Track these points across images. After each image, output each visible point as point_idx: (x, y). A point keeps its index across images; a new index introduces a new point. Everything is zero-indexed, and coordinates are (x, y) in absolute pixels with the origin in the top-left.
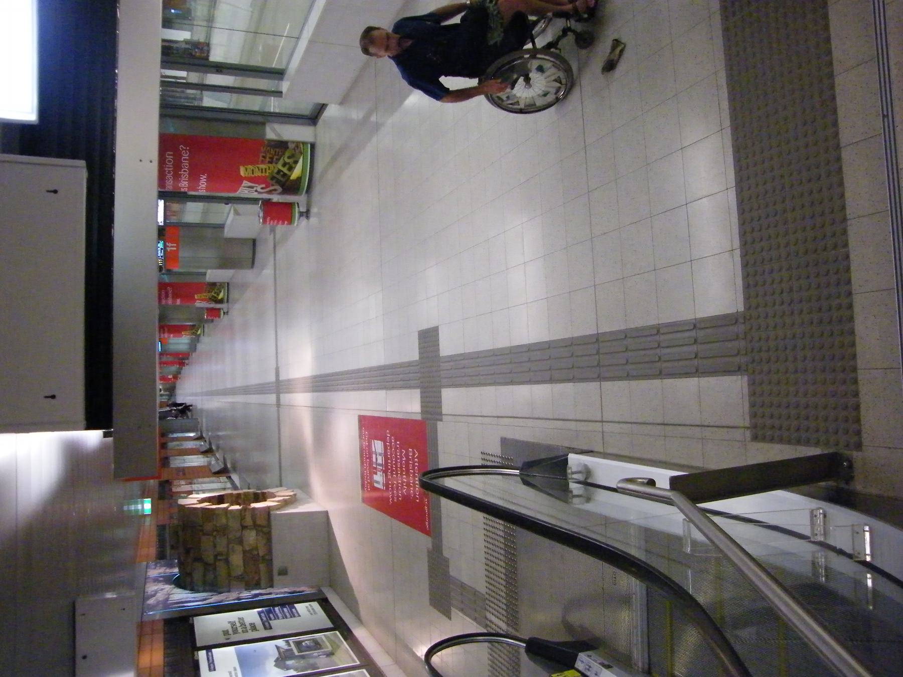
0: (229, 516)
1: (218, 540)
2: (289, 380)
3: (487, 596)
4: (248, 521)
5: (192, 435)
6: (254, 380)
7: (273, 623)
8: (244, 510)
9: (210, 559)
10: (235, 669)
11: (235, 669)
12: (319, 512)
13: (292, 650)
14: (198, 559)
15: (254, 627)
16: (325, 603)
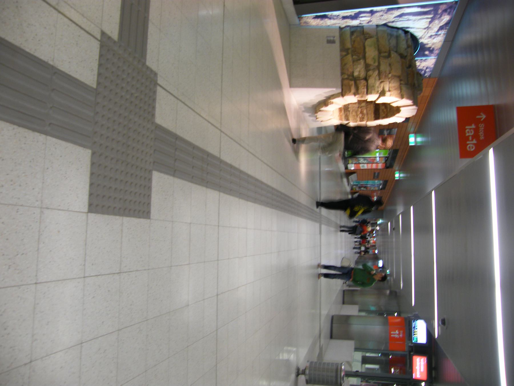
9: (394, 55)
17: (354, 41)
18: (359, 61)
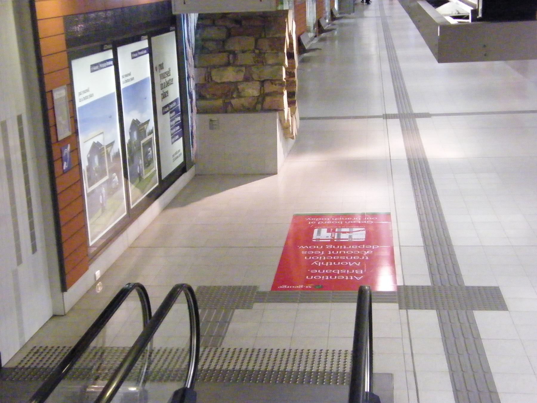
0: (277, 67)
1: (253, 55)
2: (416, 129)
3: (219, 350)
4: (269, 88)
5: (336, 6)
6: (410, 85)
7: (168, 115)
8: (282, 84)
10: (132, 79)
11: (132, 79)
12: (276, 165)
13: (145, 137)
14: (229, 35)
15: (165, 95)
16: (182, 169)
17: (214, 95)
18: (240, 90)
